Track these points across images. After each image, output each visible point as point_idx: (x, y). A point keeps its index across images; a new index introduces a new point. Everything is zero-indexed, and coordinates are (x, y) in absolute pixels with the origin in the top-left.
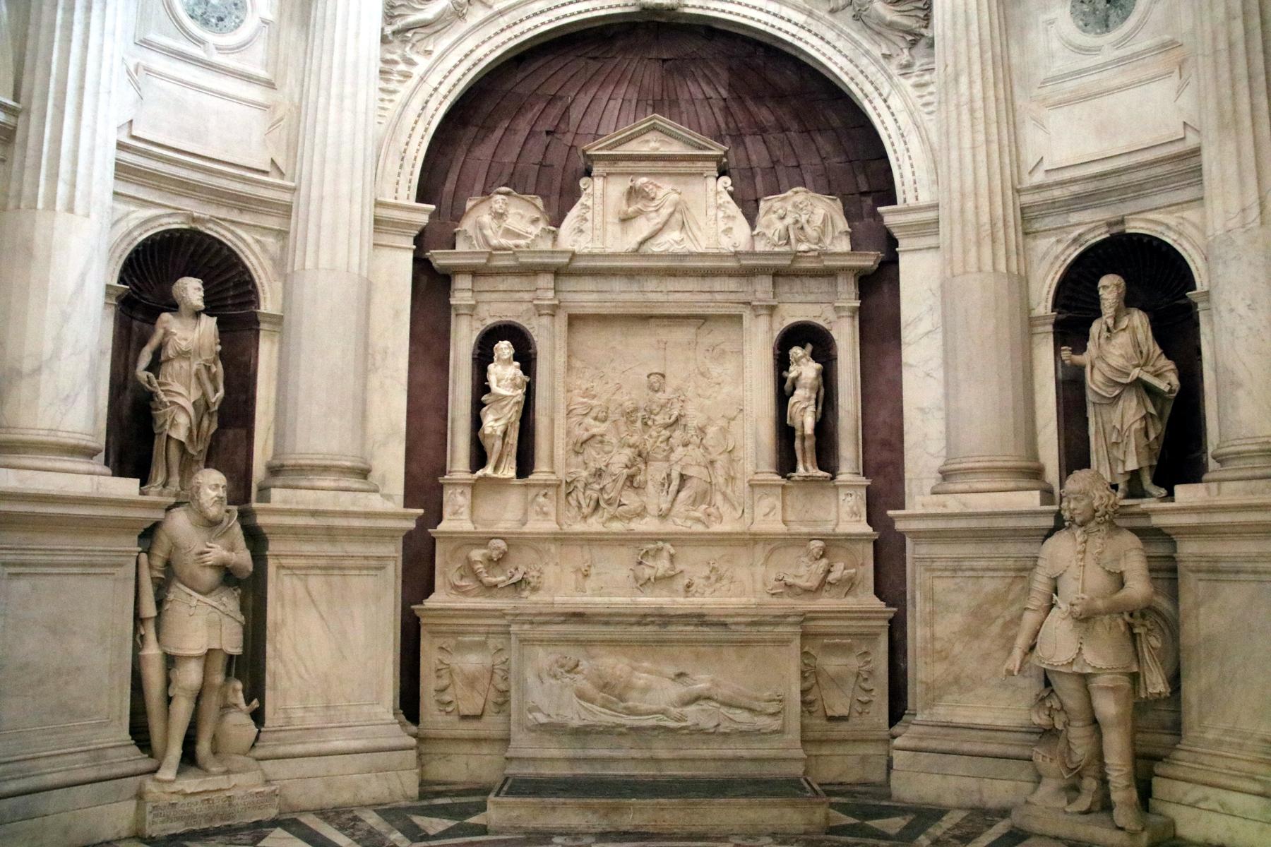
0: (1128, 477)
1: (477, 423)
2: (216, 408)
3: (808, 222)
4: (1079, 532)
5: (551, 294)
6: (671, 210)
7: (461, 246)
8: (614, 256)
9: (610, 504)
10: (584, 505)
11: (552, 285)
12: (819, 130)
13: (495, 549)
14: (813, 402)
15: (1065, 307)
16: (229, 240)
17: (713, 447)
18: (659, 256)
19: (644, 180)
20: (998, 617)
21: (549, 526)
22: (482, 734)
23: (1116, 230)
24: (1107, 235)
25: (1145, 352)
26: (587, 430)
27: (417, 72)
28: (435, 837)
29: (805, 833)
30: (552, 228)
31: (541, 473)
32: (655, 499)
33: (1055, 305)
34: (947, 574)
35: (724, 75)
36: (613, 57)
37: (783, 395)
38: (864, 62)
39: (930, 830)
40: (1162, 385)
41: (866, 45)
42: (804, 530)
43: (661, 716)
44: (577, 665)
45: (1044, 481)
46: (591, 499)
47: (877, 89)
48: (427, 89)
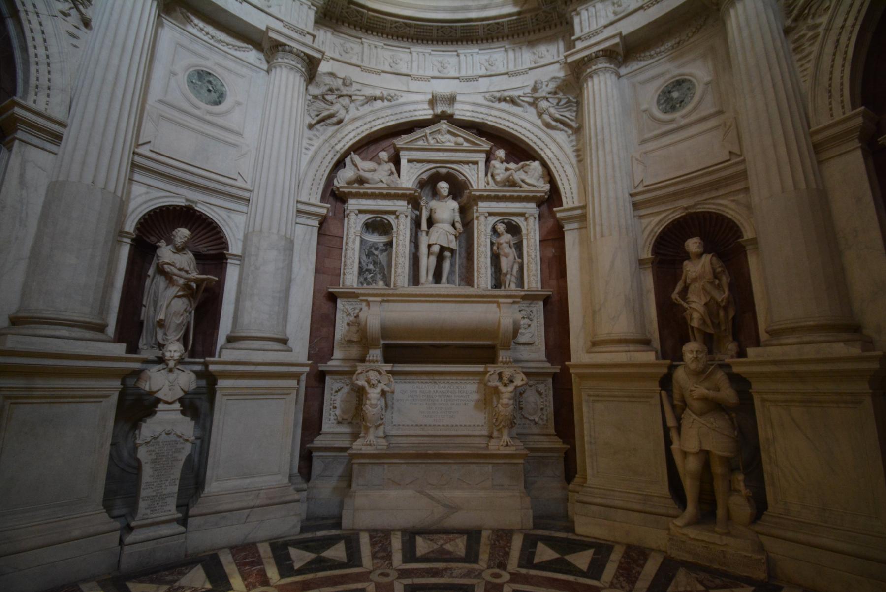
16: (714, 209)
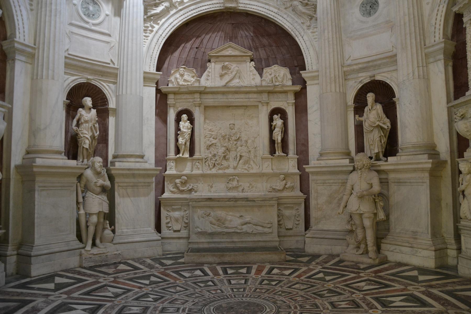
0: (375, 155)
1: (177, 140)
2: (97, 138)
3: (279, 76)
4: (359, 171)
5: (199, 100)
6: (236, 72)
7: (170, 85)
8: (219, 87)
9: (218, 165)
10: (210, 165)
11: (199, 97)
12: (282, 46)
13: (183, 179)
14: (281, 132)
15: (358, 102)
16: (99, 85)
17: (250, 147)
18: (232, 87)
19: (227, 63)
20: (336, 198)
21: (200, 172)
22: (181, 236)
23: (372, 79)
24: (370, 80)
25: (380, 116)
27: (155, 30)
28: (169, 265)
29: (279, 262)
30: (199, 79)
31: (197, 156)
32: (232, 163)
33: (355, 102)
34: (322, 184)
35: (252, 28)
36: (217, 23)
37: (271, 130)
38: (296, 25)
39: (316, 260)
40: (386, 127)
41: (296, 19)
42: (278, 171)
43: (236, 229)
44: (210, 214)
45: (351, 156)
46: (212, 163)
47: (300, 33)
48: (158, 35)
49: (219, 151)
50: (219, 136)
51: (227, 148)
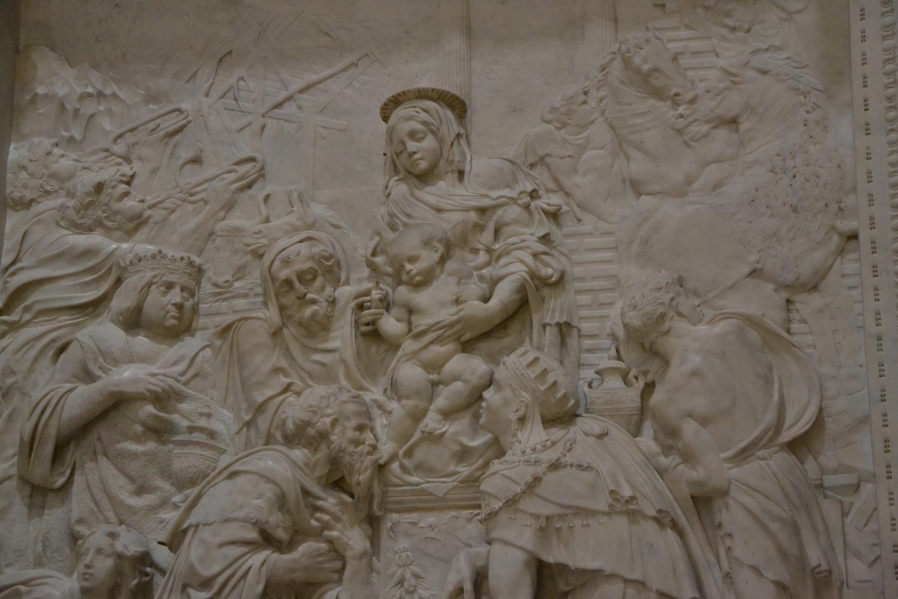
17: (704, 421)
26: (89, 377)
49: (193, 519)
50: (223, 292)
51: (334, 462)
